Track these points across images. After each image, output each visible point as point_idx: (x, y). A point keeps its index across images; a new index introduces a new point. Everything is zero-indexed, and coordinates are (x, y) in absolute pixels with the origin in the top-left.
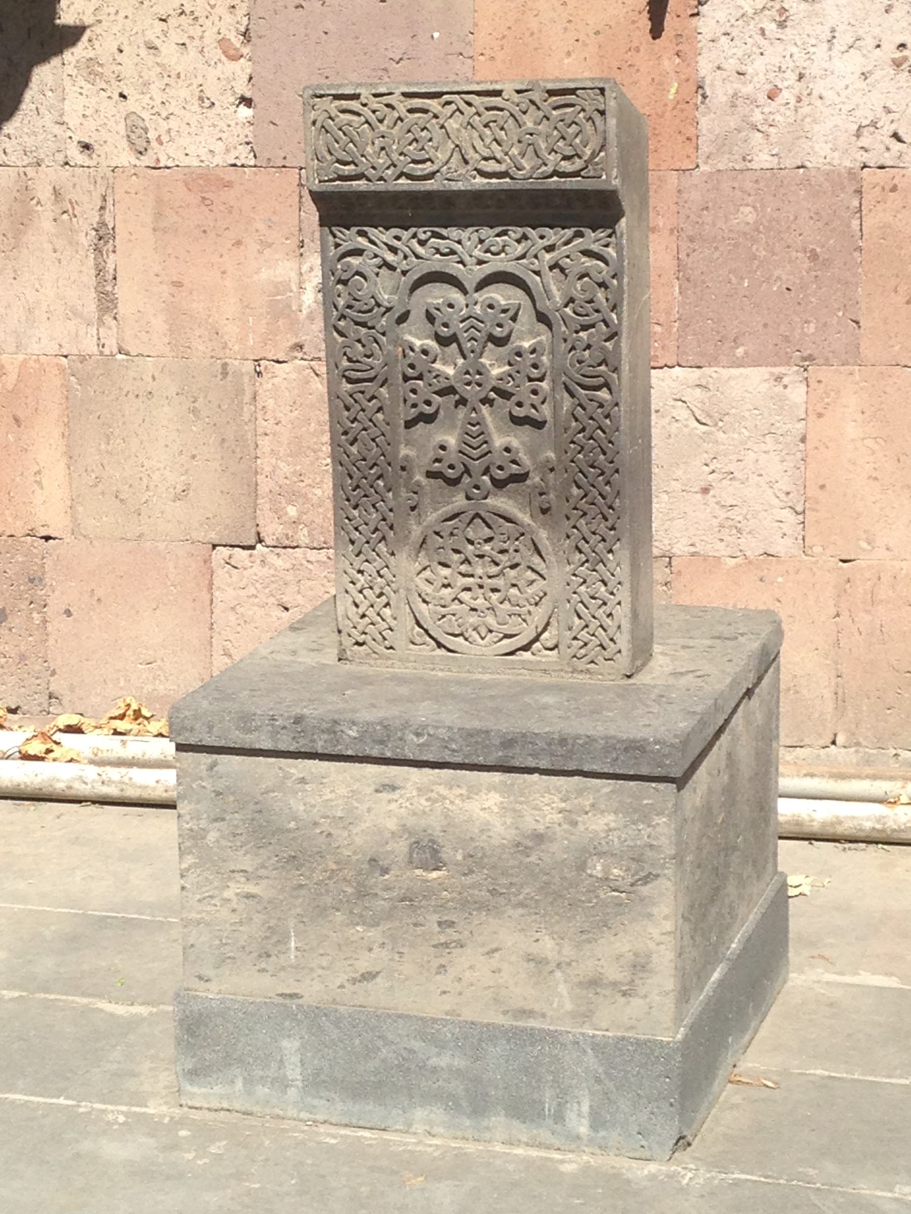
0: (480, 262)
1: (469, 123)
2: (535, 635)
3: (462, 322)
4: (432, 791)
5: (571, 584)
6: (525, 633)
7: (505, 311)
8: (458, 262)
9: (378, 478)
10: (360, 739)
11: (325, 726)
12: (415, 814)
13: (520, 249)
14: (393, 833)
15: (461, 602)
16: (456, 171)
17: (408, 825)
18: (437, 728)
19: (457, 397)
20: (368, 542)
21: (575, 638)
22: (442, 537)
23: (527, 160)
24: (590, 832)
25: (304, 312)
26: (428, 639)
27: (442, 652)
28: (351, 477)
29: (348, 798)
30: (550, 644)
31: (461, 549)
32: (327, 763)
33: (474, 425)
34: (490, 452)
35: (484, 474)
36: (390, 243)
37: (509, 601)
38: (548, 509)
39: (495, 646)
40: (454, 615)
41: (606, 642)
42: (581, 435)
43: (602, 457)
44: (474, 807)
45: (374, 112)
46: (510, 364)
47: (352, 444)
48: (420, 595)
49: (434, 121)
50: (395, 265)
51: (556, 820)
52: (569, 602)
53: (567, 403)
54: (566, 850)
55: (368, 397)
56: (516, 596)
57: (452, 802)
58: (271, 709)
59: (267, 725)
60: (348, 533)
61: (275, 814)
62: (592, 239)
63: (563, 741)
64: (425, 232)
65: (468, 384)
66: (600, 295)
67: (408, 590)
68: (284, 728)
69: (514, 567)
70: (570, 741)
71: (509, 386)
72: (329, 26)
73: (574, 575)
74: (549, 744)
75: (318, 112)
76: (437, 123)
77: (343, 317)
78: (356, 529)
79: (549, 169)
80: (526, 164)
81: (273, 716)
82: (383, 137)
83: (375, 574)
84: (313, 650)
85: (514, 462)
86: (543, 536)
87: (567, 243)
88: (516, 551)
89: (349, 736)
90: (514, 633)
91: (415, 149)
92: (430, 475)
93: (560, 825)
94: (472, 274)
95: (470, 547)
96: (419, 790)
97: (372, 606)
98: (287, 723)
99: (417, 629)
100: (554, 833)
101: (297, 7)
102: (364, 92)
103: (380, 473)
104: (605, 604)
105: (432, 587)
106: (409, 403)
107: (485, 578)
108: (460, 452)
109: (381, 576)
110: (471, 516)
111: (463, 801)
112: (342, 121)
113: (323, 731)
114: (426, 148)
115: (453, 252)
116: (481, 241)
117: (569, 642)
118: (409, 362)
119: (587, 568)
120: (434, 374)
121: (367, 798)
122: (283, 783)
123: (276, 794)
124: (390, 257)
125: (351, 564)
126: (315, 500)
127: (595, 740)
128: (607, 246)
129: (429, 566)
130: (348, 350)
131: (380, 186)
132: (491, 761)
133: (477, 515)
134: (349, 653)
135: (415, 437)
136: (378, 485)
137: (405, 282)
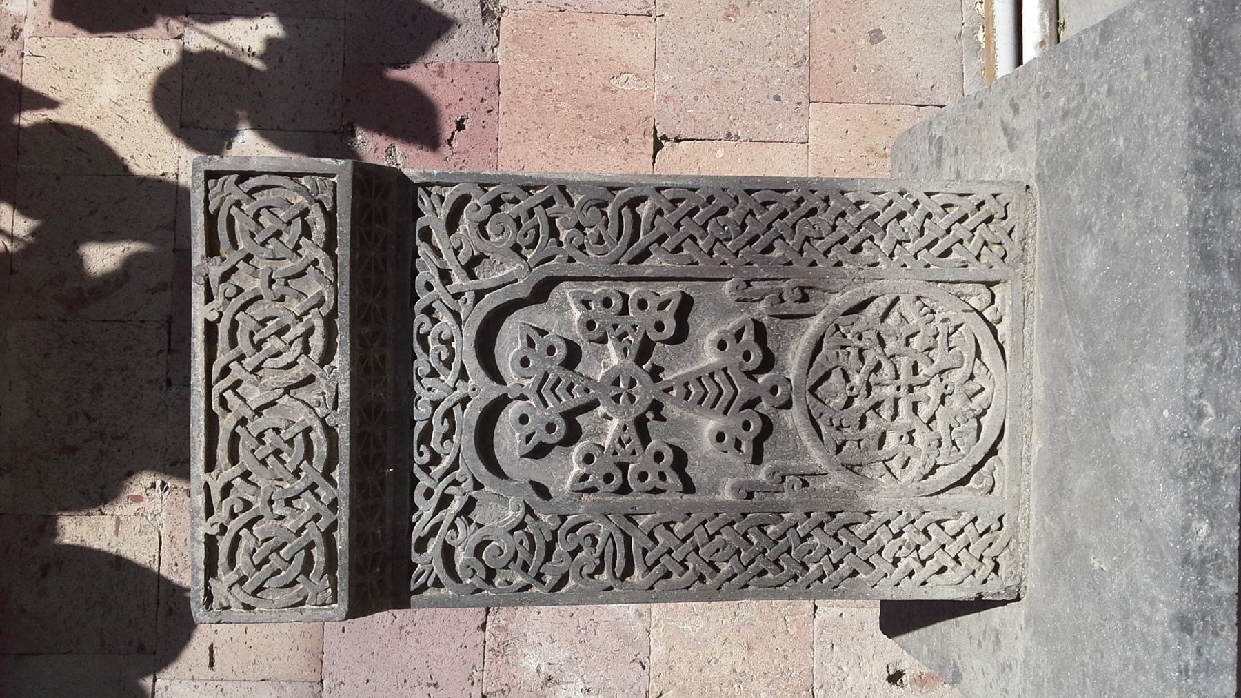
0: (463, 375)
1: (253, 372)
2: (975, 313)
3: (546, 405)
5: (903, 261)
7: (531, 344)
8: (464, 408)
10: (1211, 514)
11: (1192, 579)
13: (446, 319)
15: (933, 418)
16: (323, 394)
18: (1188, 382)
19: (650, 415)
20: (854, 551)
21: (978, 257)
22: (844, 443)
26: (984, 469)
27: (1003, 447)
28: (764, 572)
30: (987, 297)
33: (689, 393)
35: (756, 380)
36: (434, 505)
37: (930, 349)
38: (802, 288)
39: (991, 370)
40: (951, 429)
41: (983, 214)
42: (700, 242)
43: (729, 215)
45: (233, 515)
46: (603, 340)
47: (718, 570)
48: (925, 477)
49: (249, 425)
50: (466, 498)
52: (928, 266)
53: (657, 262)
55: (651, 543)
56: (923, 338)
58: (1162, 677)
60: (842, 579)
62: (433, 215)
63: (1200, 168)
64: (421, 454)
65: (632, 398)
66: (508, 210)
67: (920, 492)
68: (1199, 651)
70: (1200, 154)
71: (634, 339)
72: (362, 677)
73: (892, 255)
74: (1206, 190)
75: (232, 600)
76: (253, 420)
77: (539, 577)
78: (836, 566)
79: (321, 255)
81: (1181, 672)
82: (271, 502)
83: (899, 541)
84: (997, 642)
85: (738, 335)
86: (839, 300)
87: (438, 253)
88: (860, 338)
89: (1208, 536)
90: (974, 339)
91: (290, 455)
92: (757, 459)
94: (482, 389)
95: (857, 403)
97: (943, 547)
98: (1192, 648)
99: (971, 484)
102: (206, 527)
104: (929, 216)
106: (660, 485)
107: (898, 382)
108: (725, 413)
109: (901, 533)
110: (815, 400)
112: (245, 564)
113: (1202, 582)
114: (288, 437)
115: (449, 414)
116: (434, 373)
117: (983, 266)
118: (601, 481)
119: (882, 239)
120: (618, 446)
124: (455, 506)
127: (1197, 112)
128: (442, 199)
129: (884, 461)
130: (586, 571)
131: (344, 506)
133: (813, 390)
134: (1010, 583)
135: (706, 479)
136: (774, 532)
137: (491, 486)
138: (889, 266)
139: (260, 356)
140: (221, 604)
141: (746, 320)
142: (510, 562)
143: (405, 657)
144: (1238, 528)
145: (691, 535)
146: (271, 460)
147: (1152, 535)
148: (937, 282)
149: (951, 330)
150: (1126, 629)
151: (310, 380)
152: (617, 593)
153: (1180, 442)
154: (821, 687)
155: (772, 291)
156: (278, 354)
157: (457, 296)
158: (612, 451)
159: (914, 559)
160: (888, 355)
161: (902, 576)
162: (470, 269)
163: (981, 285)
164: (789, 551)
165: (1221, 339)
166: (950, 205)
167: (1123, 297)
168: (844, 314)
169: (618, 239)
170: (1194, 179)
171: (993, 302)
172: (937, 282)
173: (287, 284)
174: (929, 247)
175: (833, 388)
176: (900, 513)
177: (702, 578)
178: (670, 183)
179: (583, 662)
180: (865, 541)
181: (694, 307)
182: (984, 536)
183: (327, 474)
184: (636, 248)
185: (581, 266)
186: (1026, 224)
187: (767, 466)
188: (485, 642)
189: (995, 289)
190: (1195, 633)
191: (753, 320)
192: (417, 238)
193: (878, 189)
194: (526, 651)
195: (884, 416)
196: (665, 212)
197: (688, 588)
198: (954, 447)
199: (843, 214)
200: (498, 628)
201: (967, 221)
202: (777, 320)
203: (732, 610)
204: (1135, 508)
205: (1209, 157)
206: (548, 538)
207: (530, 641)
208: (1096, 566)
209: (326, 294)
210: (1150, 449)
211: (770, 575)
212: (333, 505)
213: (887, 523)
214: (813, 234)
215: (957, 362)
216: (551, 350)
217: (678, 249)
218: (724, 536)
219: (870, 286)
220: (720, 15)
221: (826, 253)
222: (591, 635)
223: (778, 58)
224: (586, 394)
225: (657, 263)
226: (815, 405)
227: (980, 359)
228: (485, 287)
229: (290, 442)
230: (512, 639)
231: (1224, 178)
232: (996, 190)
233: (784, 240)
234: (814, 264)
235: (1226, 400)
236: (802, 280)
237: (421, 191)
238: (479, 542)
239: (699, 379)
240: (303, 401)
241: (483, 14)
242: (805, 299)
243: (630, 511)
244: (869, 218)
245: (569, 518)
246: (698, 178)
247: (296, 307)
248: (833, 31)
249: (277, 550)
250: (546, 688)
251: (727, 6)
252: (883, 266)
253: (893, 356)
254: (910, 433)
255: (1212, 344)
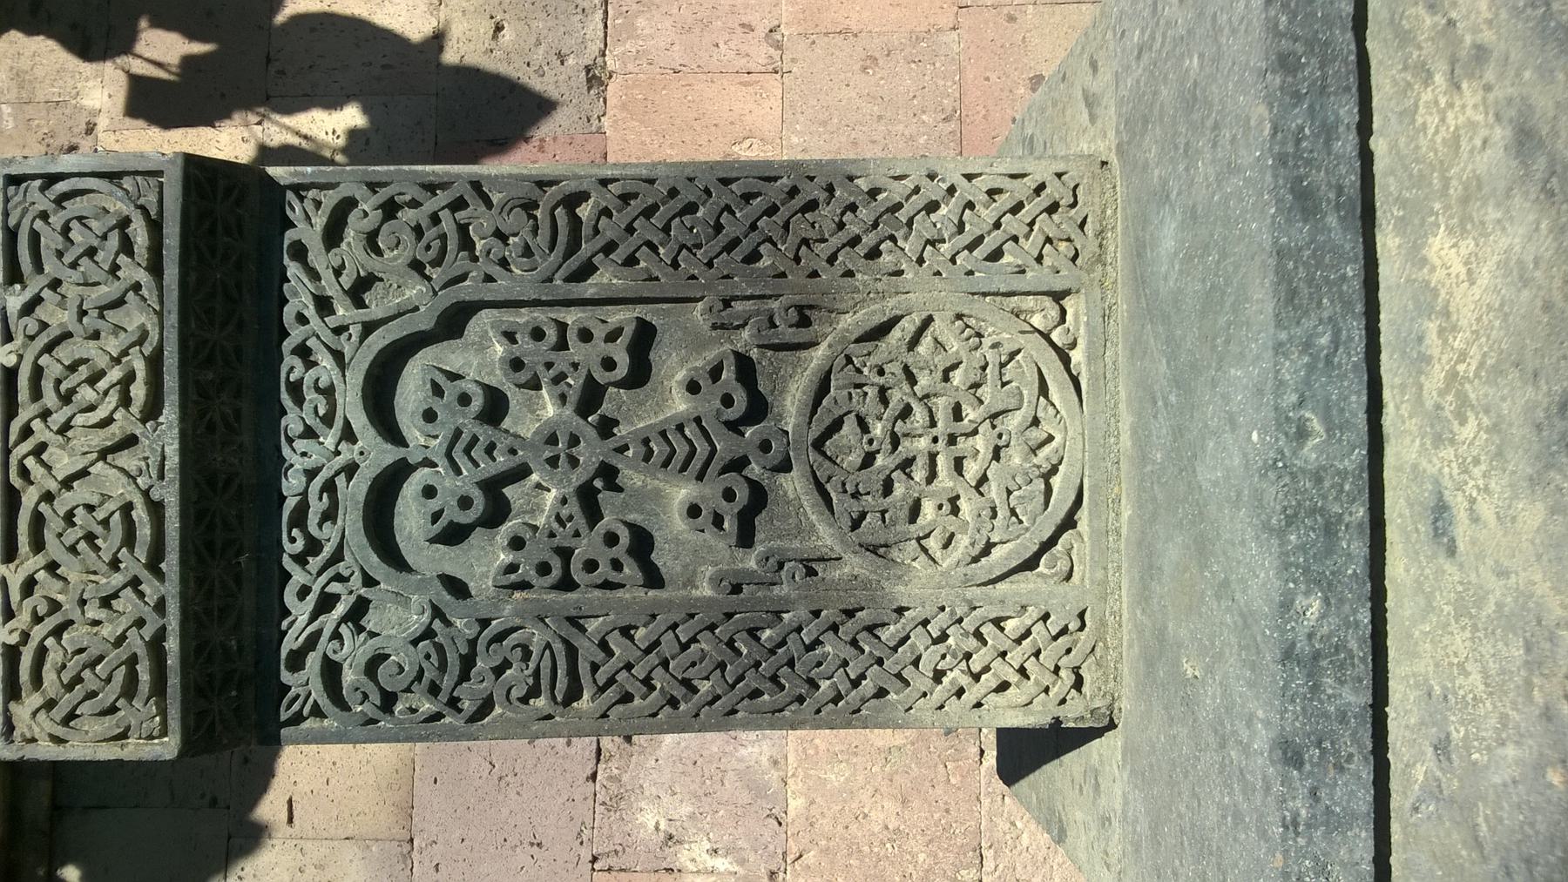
0: (348, 435)
2: (1036, 334)
3: (458, 472)
4: (1438, 407)
5: (936, 268)
6: (1033, 353)
7: (438, 391)
9: (758, 639)
10: (1326, 586)
12: (1499, 454)
13: (325, 361)
14: (1553, 511)
15: (983, 479)
17: (1529, 471)
18: (1280, 384)
19: (598, 484)
20: (880, 662)
21: (1039, 259)
22: (863, 515)
23: (130, 322)
24: (1497, 15)
25: (736, 868)
26: (1059, 547)
27: (1083, 516)
28: (756, 694)
29: (1475, 628)
30: (1054, 313)
31: (882, 477)
32: (1392, 684)
34: (698, 420)
35: (743, 435)
36: (310, 607)
37: (976, 386)
38: (800, 309)
39: (1063, 412)
40: (1009, 493)
41: (1043, 201)
42: (661, 251)
44: (1468, 302)
45: (37, 619)
46: (535, 385)
47: (695, 690)
48: (976, 560)
50: (353, 598)
51: (1478, 98)
52: (970, 273)
53: (606, 279)
54: (1545, 74)
57: (1463, 355)
58: (1263, 834)
59: (1310, 841)
61: (1532, 825)
62: (307, 227)
64: (293, 540)
65: (574, 462)
66: (407, 215)
68: (1314, 793)
69: (912, 380)
71: (574, 381)
72: (457, 835)
74: (1298, 97)
75: (36, 730)
77: (453, 703)
78: (855, 684)
79: (143, 276)
80: (135, 317)
81: (1286, 827)
82: (83, 602)
83: (941, 648)
84: (1097, 786)
86: (851, 322)
87: (314, 275)
88: (881, 372)
89: (1323, 617)
90: (1036, 369)
91: (105, 540)
92: (746, 538)
93: (1488, 88)
94: (375, 454)
95: (880, 460)
96: (1438, 441)
97: (1003, 654)
98: (1303, 792)
99: (1041, 569)
100: (1510, 101)
101: (437, 870)
103: (745, 634)
104: (970, 205)
105: (958, 536)
106: (614, 577)
107: (934, 431)
108: (700, 477)
109: (944, 637)
110: (820, 459)
111: (1455, 329)
113: (1316, 688)
116: (309, 433)
118: (533, 573)
119: (906, 238)
120: (555, 525)
121: (1473, 577)
122: (1452, 801)
123: (1480, 820)
124: (340, 609)
125: (925, 695)
126: (930, 861)
128: (318, 204)
129: (919, 539)
130: (515, 694)
131: (173, 607)
132: (1351, 244)
133: (818, 445)
134: (1098, 703)
135: (679, 569)
136: (770, 638)
137: (387, 582)
138: (916, 274)
139: (67, 411)
140: (23, 735)
141: (724, 352)
142: (413, 682)
143: (505, 811)
144: (1369, 605)
145: (657, 643)
146: (82, 546)
147: (1246, 620)
148: (985, 294)
149: (1004, 358)
150: (1223, 766)
151: (130, 441)
152: (558, 723)
153: (1272, 475)
154: (990, 847)
155: (758, 313)
156: (91, 408)
157: (338, 331)
158: (547, 532)
159: (962, 671)
160: (919, 394)
161: (946, 695)
162: (357, 293)
163: (1045, 298)
164: (791, 663)
165: (1330, 318)
166: (999, 191)
167: (1204, 281)
168: (858, 341)
169: (552, 249)
170: (1278, 80)
171: (1063, 320)
172: (985, 294)
173: (102, 316)
174: (971, 247)
175: (845, 441)
176: (943, 609)
177: (673, 702)
178: (617, 173)
179: (708, 819)
180: (895, 649)
181: (657, 339)
182: (1060, 640)
183: (154, 565)
184: (574, 263)
185: (503, 286)
186: (1104, 212)
187: (759, 548)
188: (595, 795)
189: (1067, 303)
190: (1308, 767)
191: (737, 354)
192: (286, 256)
193: (898, 172)
194: (643, 804)
195: (917, 479)
196: (614, 213)
197: (654, 715)
198: (1014, 519)
199: (853, 208)
200: (610, 778)
201: (1023, 211)
202: (769, 353)
203: (883, 755)
204: (1225, 583)
205: (1299, 48)
206: (464, 650)
207: (647, 793)
208: (1190, 672)
209: (149, 327)
210: (1239, 495)
211: (766, 697)
212: (160, 607)
213: (925, 623)
214: (811, 234)
215: (1013, 403)
216: (465, 399)
217: (631, 261)
218: (704, 646)
219: (891, 302)
220: (857, 67)
221: (832, 260)
222: (718, 786)
223: (924, 112)
224: (511, 457)
225: (605, 281)
226: (821, 465)
227: (1046, 397)
228: (374, 317)
229: (105, 523)
230: (627, 791)
231: (1324, 78)
232: (1061, 167)
233: (775, 245)
234: (814, 274)
235: (1342, 410)
236: (798, 297)
237: (290, 195)
238: (369, 656)
239: (663, 434)
240: (122, 470)
241: (589, 80)
242: (804, 322)
243: (573, 613)
244: (887, 210)
245: (494, 623)
246: (654, 165)
247: (113, 345)
248: (987, 79)
249: (92, 665)
250: (666, 849)
251: (864, 57)
252: (909, 275)
253: (927, 396)
254: (954, 500)
255: (1316, 327)
